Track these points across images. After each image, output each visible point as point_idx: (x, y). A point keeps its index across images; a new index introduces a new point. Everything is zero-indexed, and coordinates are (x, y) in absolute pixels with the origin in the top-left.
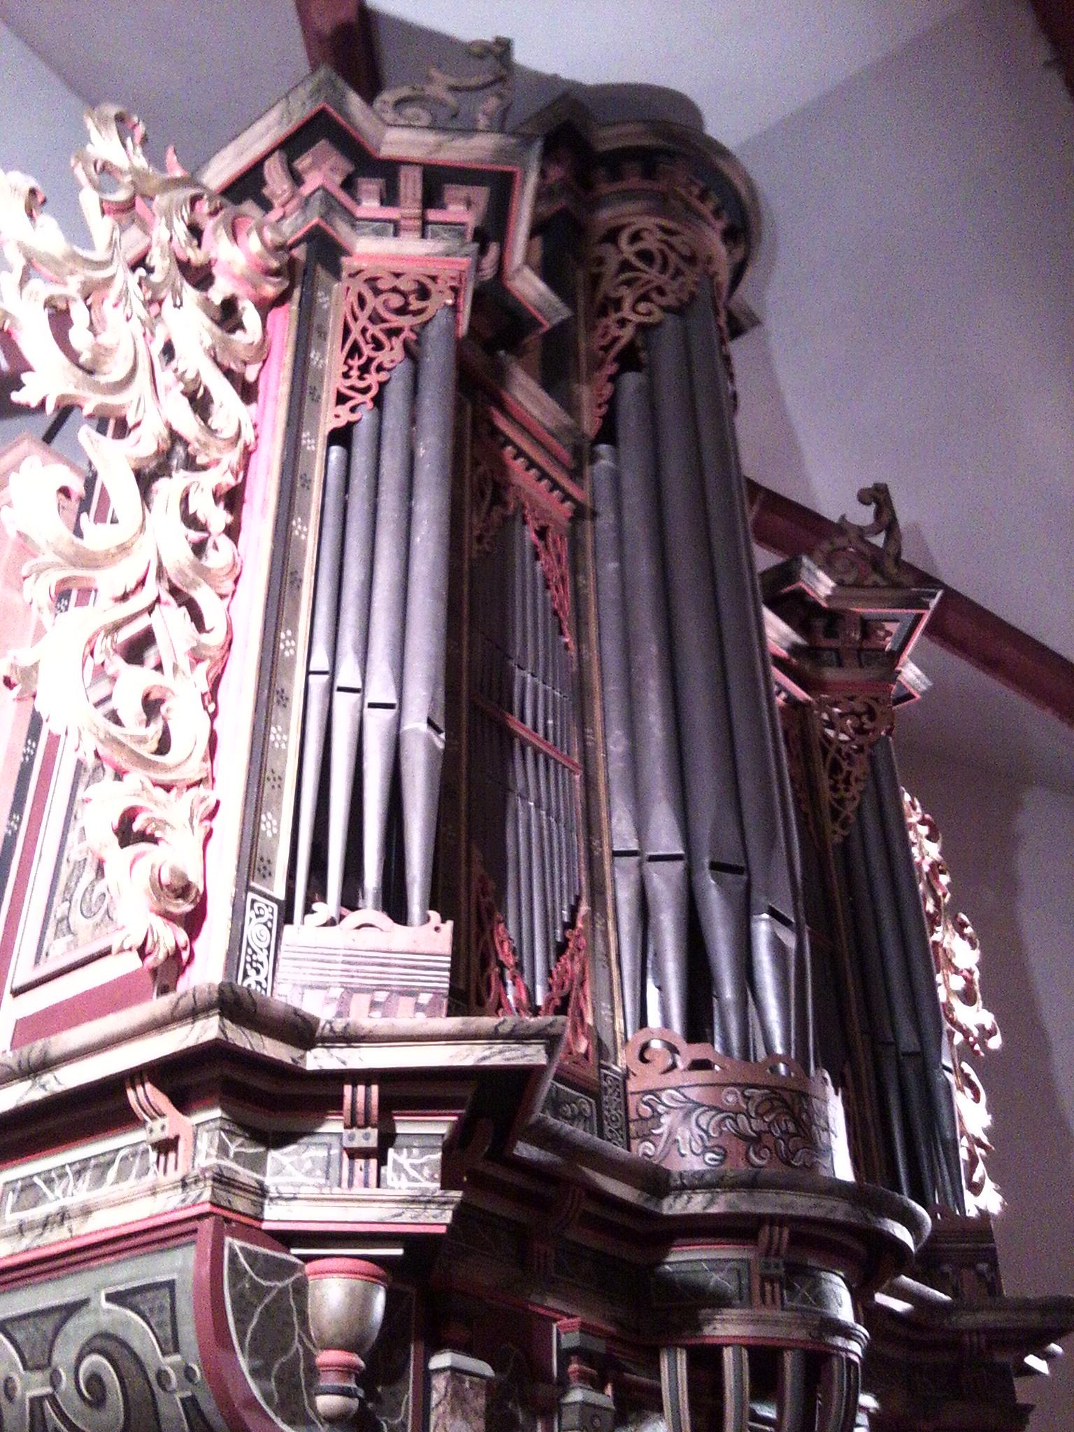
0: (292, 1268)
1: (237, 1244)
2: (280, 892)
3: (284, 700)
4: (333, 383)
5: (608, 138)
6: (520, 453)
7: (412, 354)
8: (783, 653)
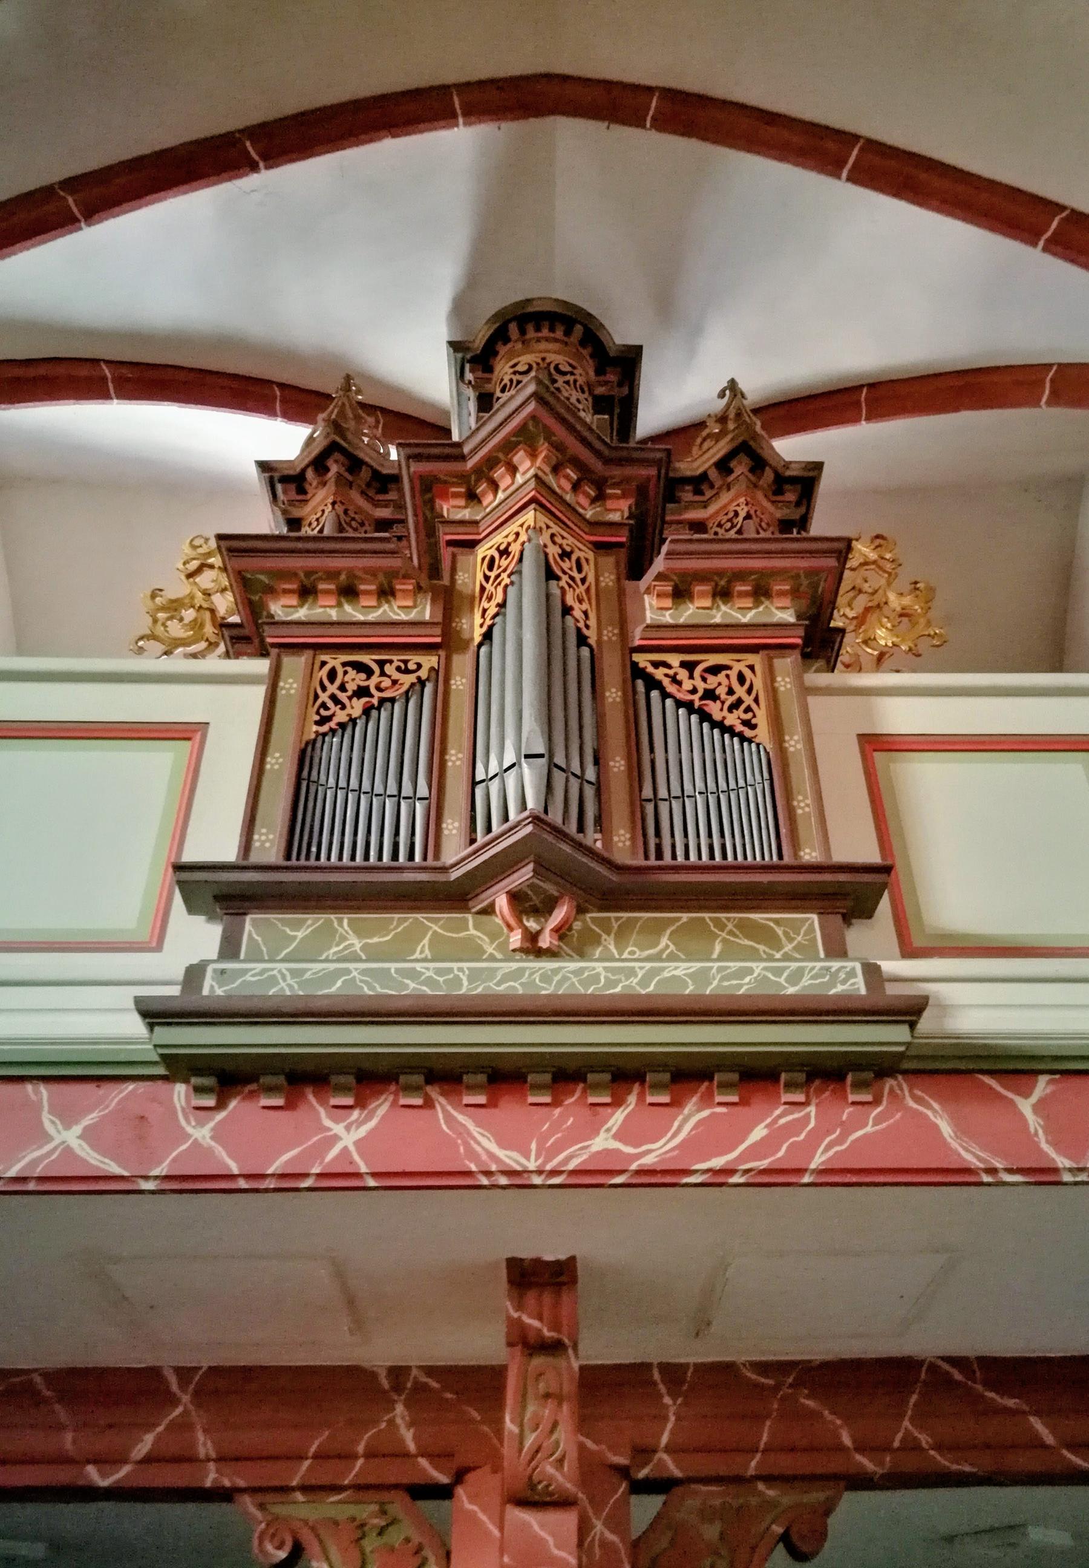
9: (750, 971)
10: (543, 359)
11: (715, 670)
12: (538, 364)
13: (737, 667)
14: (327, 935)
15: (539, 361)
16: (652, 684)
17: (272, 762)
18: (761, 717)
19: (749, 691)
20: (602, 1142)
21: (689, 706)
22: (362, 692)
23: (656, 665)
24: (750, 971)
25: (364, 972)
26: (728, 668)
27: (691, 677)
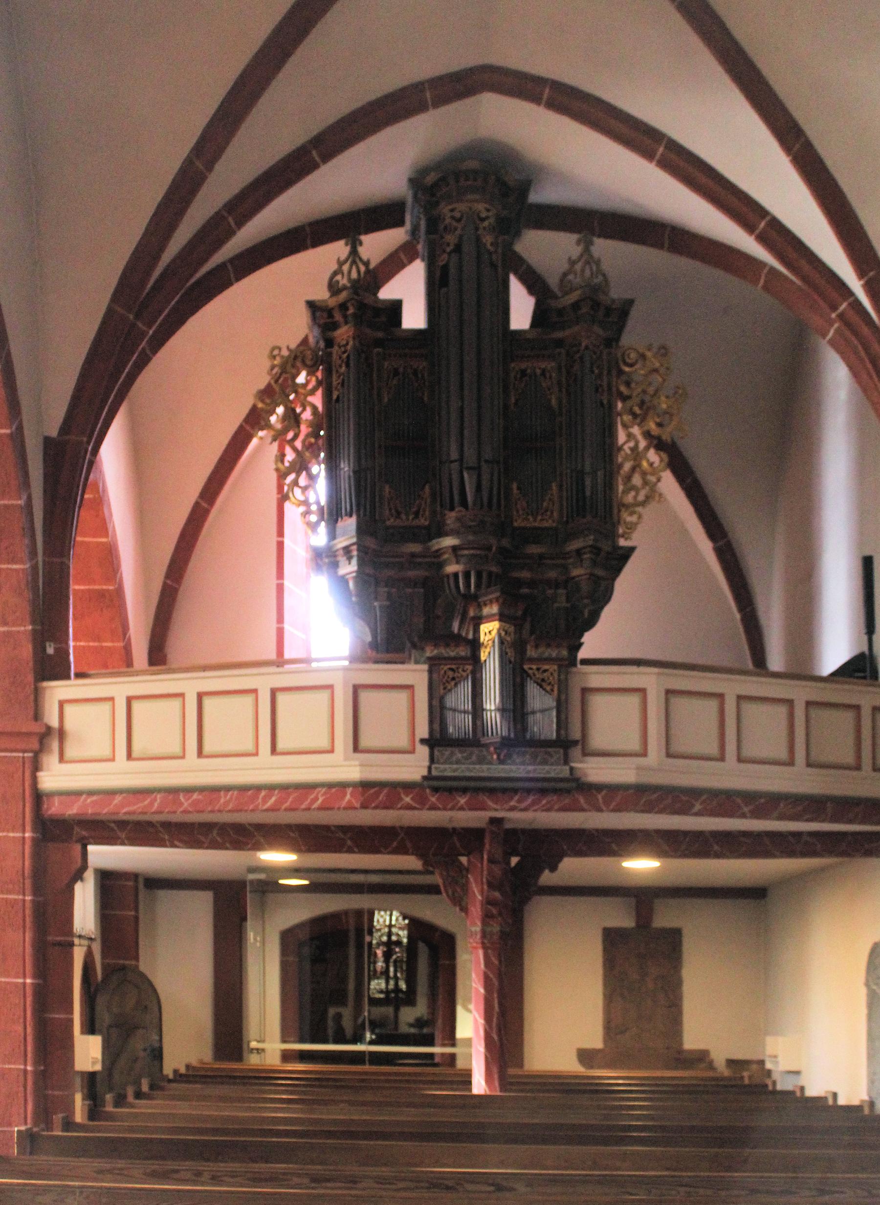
5: (431, 179)
11: (545, 671)
13: (551, 670)
16: (528, 675)
22: (453, 679)
23: (531, 669)
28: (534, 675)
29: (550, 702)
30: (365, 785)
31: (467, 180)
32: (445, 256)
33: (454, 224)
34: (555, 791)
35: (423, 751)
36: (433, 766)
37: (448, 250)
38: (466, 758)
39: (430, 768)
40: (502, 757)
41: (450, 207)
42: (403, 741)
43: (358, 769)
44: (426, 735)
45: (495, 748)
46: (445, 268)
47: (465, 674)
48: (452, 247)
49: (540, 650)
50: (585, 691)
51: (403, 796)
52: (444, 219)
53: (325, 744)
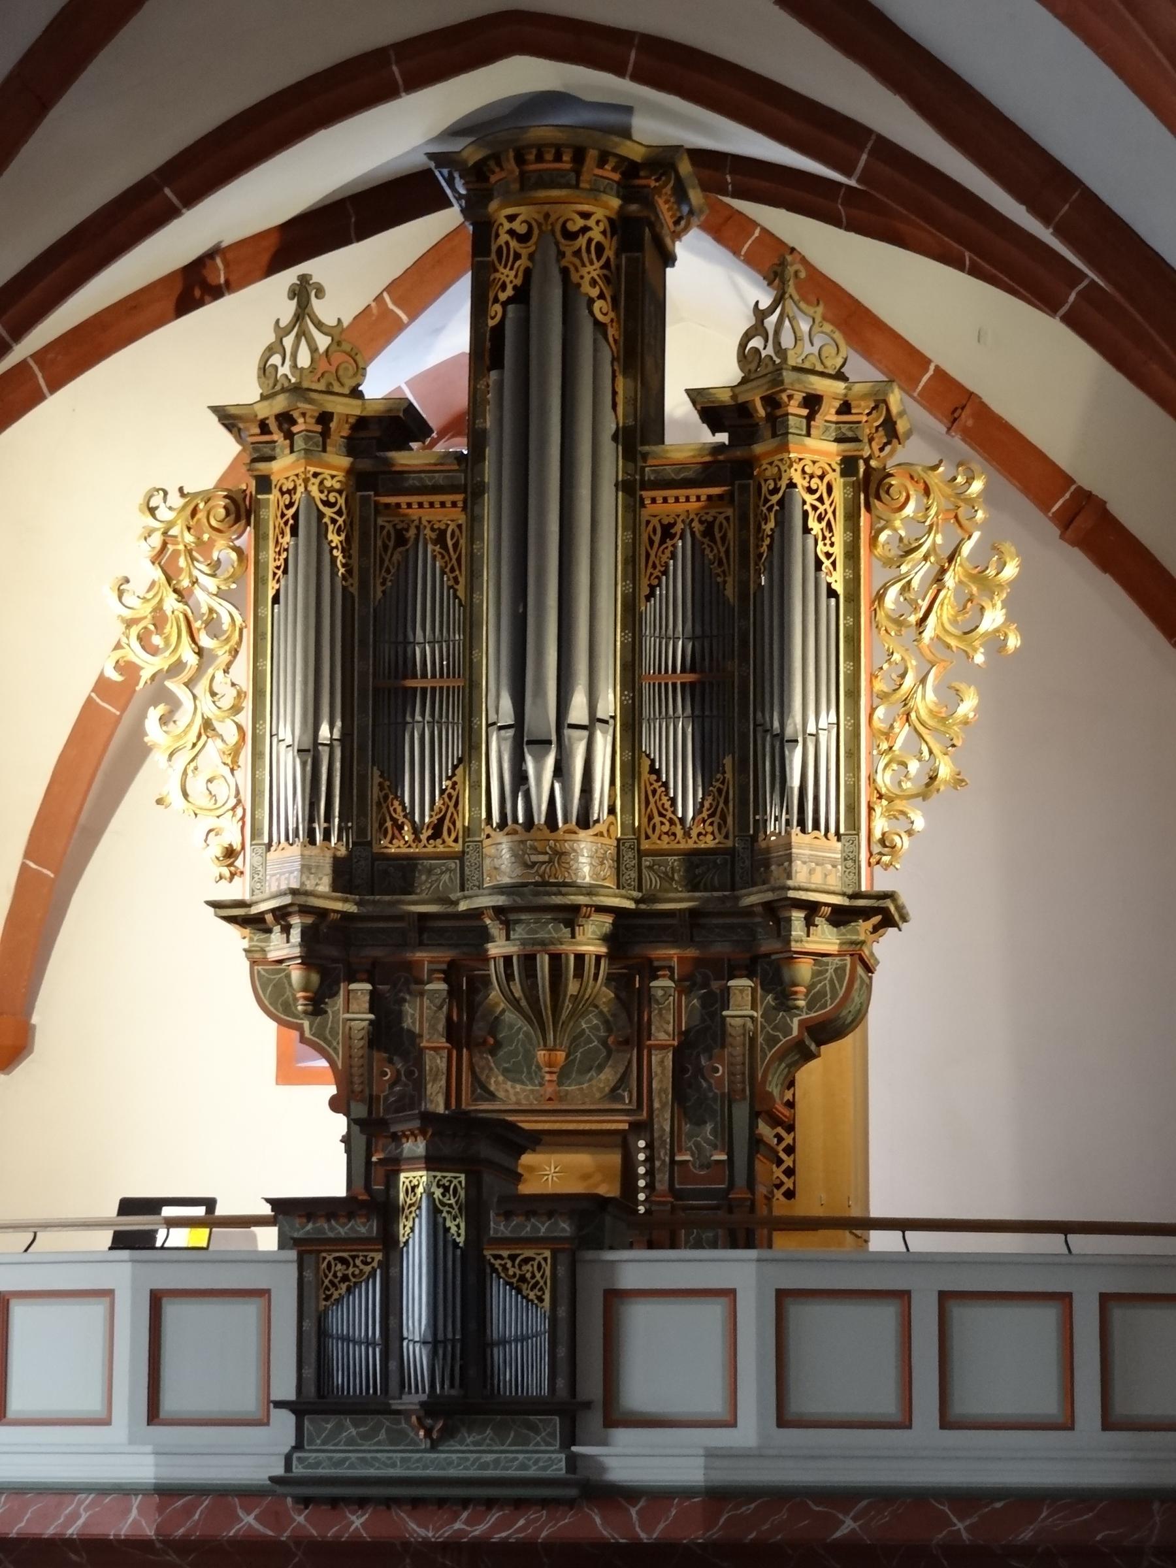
0: (284, 970)
1: (260, 968)
2: (266, 840)
3: (262, 754)
4: (272, 565)
6: (409, 505)
7: (294, 532)
8: (708, 459)
9: (517, 1459)
10: (547, 216)
11: (527, 1260)
12: (539, 225)
13: (539, 1258)
14: (340, 1428)
15: (541, 220)
17: (306, 1324)
18: (547, 1297)
19: (542, 1277)
20: (458, 1525)
21: (511, 1284)
22: (345, 1278)
23: (497, 1257)
24: (517, 1459)
25: (358, 1458)
26: (534, 1259)
27: (513, 1266)
28: (505, 1269)
29: (537, 1321)
30: (165, 1493)
31: (540, 158)
32: (498, 308)
33: (514, 244)
34: (544, 1503)
35: (285, 1421)
36: (295, 1455)
37: (503, 297)
38: (365, 1437)
39: (288, 1459)
40: (435, 1436)
41: (510, 211)
42: (248, 1402)
43: (150, 1459)
44: (290, 1394)
45: (418, 1419)
46: (499, 329)
47: (367, 1269)
48: (509, 292)
49: (515, 1221)
50: (615, 1297)
51: (241, 1513)
52: (497, 235)
53: (93, 1404)
